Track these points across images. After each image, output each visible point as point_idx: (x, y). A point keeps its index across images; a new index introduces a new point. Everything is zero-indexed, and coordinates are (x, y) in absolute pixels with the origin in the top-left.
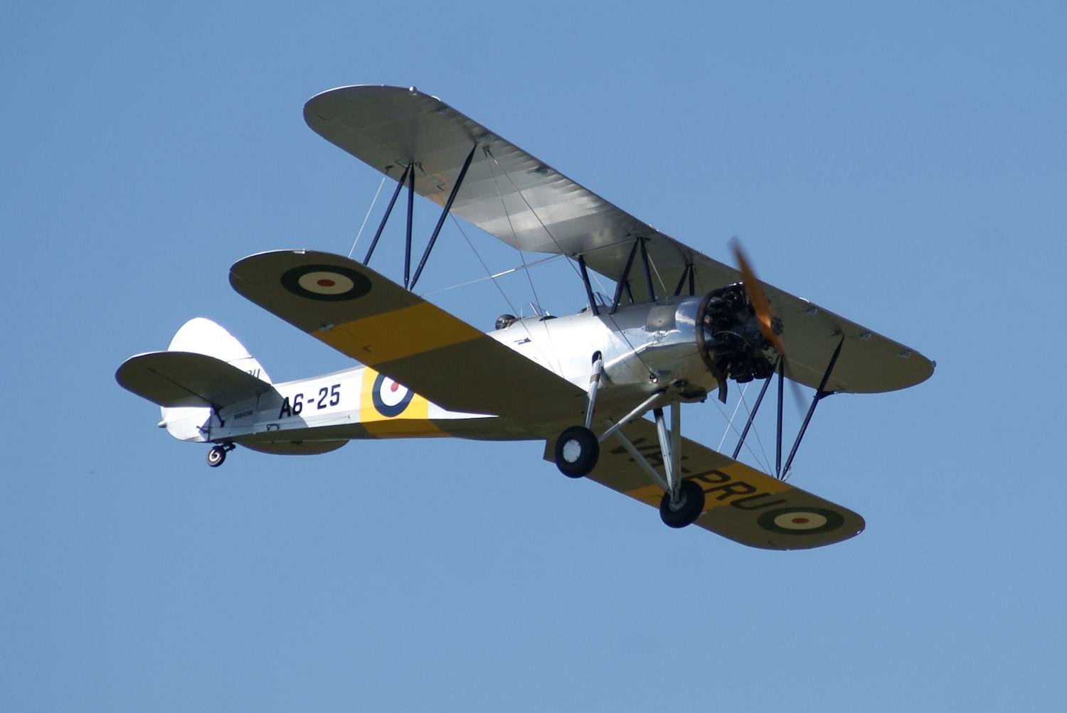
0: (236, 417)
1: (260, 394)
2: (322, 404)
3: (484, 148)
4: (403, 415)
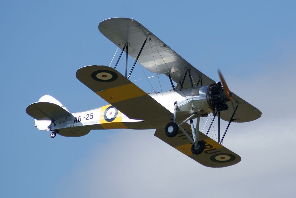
0: (59, 123)
1: (67, 117)
2: (87, 119)
3: (149, 39)
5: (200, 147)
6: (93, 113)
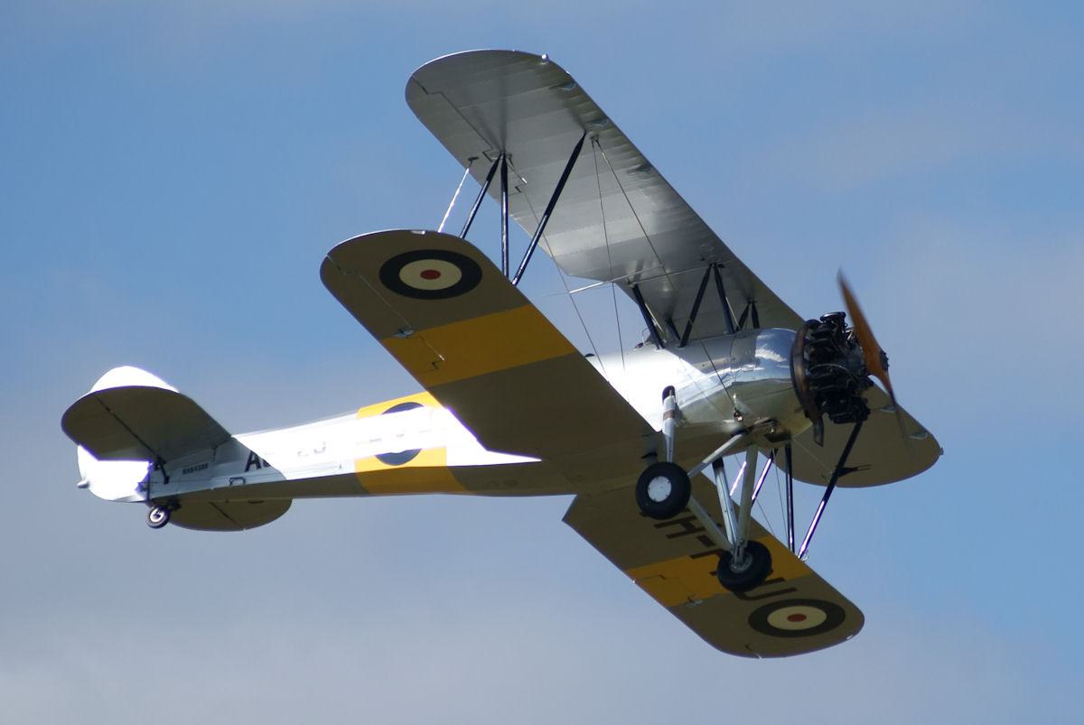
0: (185, 472)
3: (592, 138)
5: (751, 567)
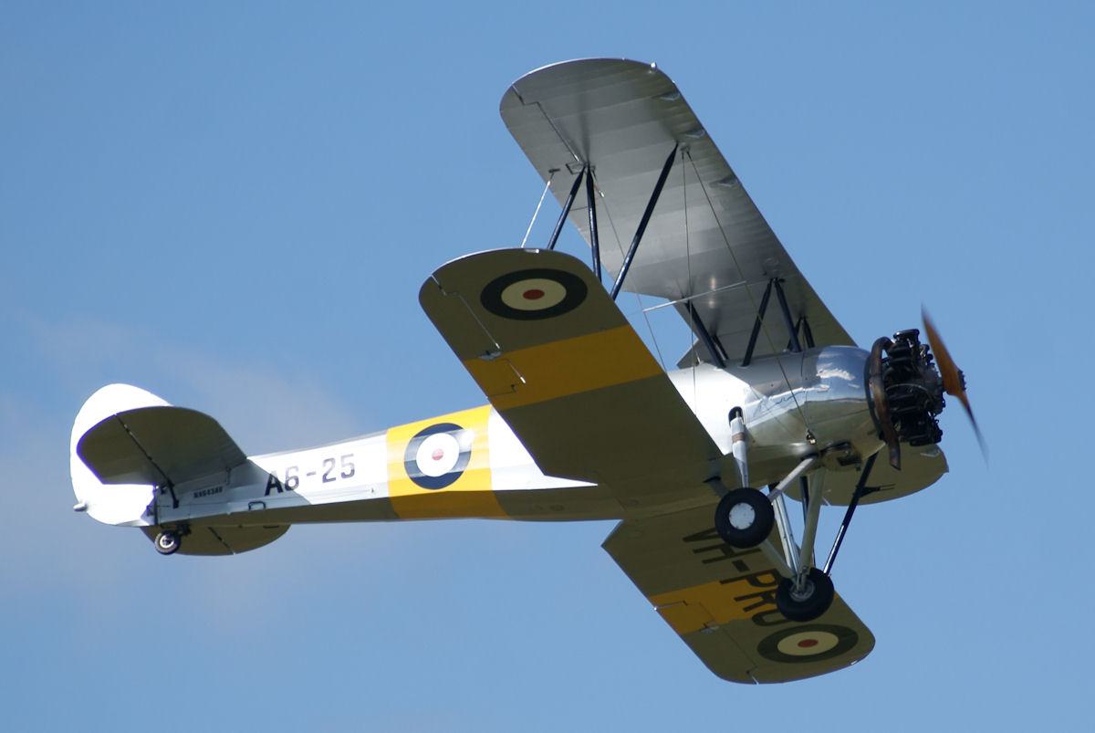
0: (196, 496)
1: (230, 469)
3: (682, 149)
4: (455, 487)
6: (352, 455)
